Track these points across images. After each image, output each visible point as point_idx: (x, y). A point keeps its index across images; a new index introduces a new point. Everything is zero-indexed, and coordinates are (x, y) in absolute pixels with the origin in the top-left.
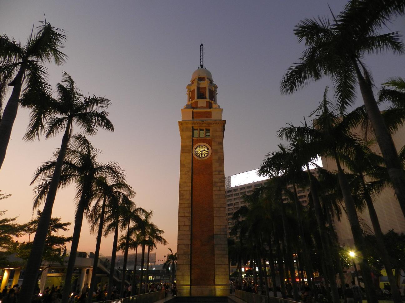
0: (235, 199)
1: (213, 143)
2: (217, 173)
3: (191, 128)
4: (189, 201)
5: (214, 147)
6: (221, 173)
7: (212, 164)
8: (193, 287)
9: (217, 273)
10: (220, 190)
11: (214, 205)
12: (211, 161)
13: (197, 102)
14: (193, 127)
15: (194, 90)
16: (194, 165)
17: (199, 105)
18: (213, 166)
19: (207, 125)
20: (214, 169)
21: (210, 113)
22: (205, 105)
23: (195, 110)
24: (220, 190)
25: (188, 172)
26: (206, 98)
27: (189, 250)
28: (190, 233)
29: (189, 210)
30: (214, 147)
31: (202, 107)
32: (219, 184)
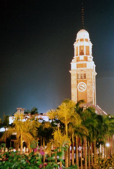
1: (87, 82)
2: (89, 98)
6: (91, 99)
7: (87, 94)
12: (87, 92)
16: (78, 95)
17: (80, 60)
20: (88, 97)
22: (83, 59)
23: (79, 63)
25: (76, 98)
31: (82, 60)
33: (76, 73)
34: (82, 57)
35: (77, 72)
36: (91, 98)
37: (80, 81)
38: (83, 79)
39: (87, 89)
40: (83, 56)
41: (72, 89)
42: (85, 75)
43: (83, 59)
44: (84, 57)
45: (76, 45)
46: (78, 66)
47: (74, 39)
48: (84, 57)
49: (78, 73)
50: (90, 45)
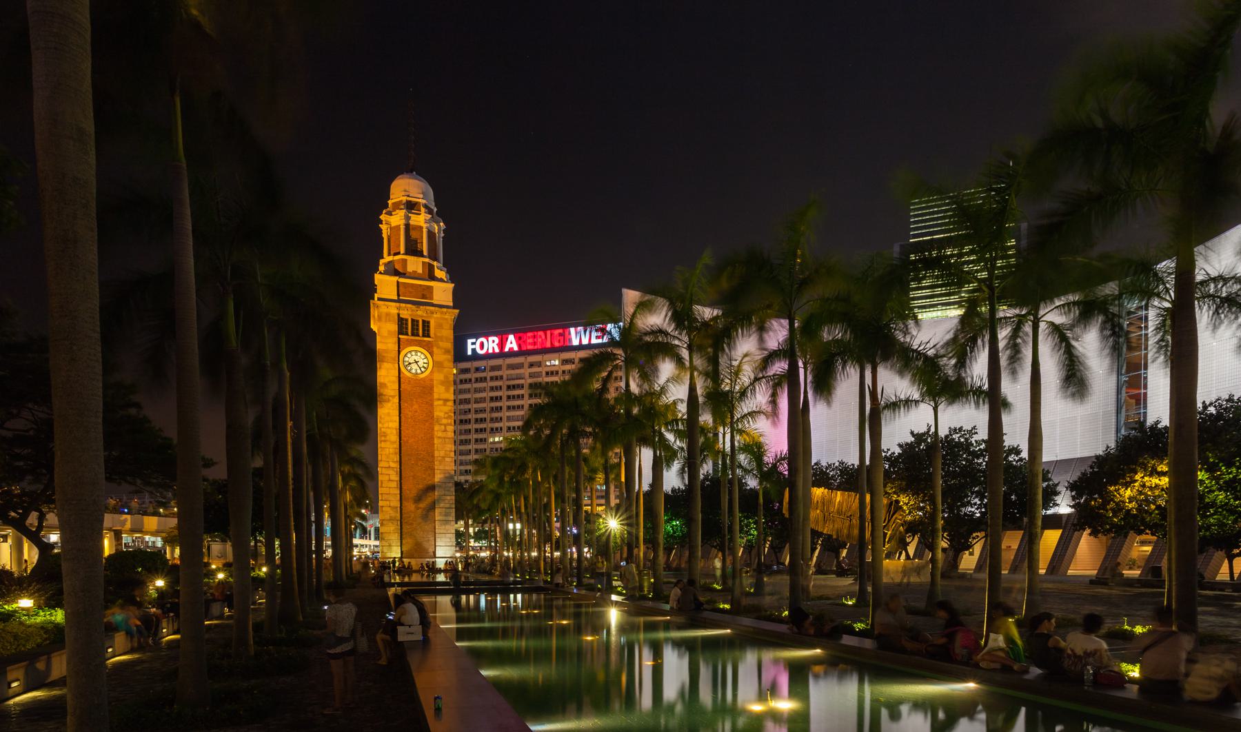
1: (435, 349)
2: (441, 402)
5: (436, 358)
10: (445, 431)
11: (436, 453)
12: (432, 380)
13: (405, 261)
15: (398, 227)
17: (410, 269)
18: (435, 390)
20: (436, 396)
22: (420, 271)
24: (445, 431)
26: (422, 256)
30: (436, 358)
32: (445, 421)
33: (396, 311)
34: (415, 264)
35: (398, 308)
36: (446, 400)
37: (411, 343)
39: (432, 372)
40: (422, 259)
42: (426, 324)
43: (420, 271)
48: (424, 263)
49: (405, 314)
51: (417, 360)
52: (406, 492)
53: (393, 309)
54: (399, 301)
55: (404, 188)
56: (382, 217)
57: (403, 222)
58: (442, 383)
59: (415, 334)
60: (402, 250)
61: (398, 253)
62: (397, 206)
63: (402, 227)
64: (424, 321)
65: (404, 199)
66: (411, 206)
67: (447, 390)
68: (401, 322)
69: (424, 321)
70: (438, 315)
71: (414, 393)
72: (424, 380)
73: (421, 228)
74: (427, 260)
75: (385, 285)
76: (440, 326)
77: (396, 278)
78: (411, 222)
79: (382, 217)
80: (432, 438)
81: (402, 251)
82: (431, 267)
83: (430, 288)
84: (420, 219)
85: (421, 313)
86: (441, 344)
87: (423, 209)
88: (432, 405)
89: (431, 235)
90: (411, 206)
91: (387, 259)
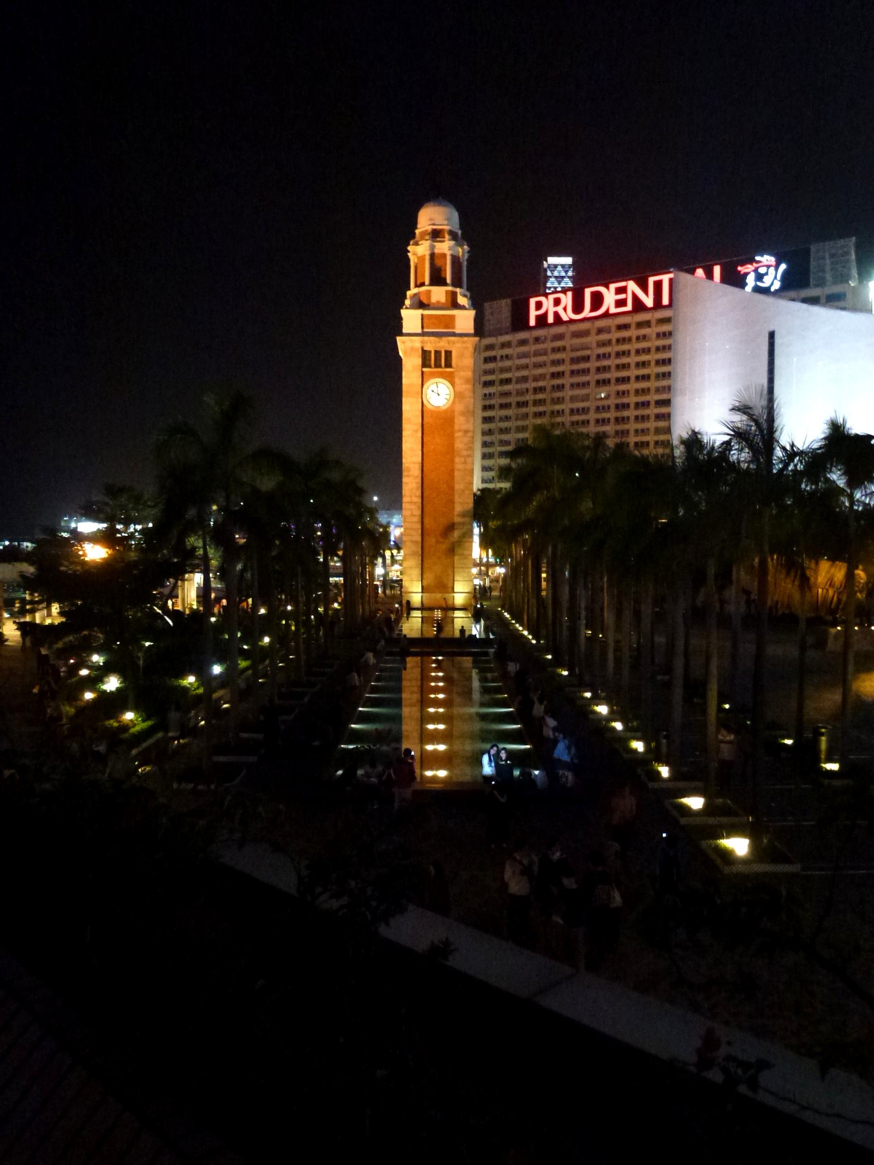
0: (518, 368)
1: (457, 381)
3: (420, 350)
4: (419, 480)
5: (458, 388)
8: (425, 594)
9: (456, 578)
10: (465, 463)
12: (453, 412)
13: (429, 292)
14: (422, 349)
19: (447, 345)
20: (456, 427)
21: (452, 318)
22: (443, 299)
24: (465, 463)
25: (416, 431)
27: (420, 550)
28: (420, 527)
29: (419, 493)
32: (465, 453)
34: (439, 294)
37: (433, 375)
38: (440, 366)
41: (404, 399)
42: (448, 354)
44: (447, 292)
45: (418, 251)
46: (425, 320)
47: (408, 234)
48: (447, 292)
50: (463, 251)
51: (439, 394)
52: (427, 525)
53: (417, 342)
54: (423, 334)
55: (430, 217)
56: (409, 248)
57: (427, 253)
58: (463, 414)
59: (438, 365)
60: (427, 282)
61: (423, 284)
62: (423, 234)
63: (427, 258)
64: (446, 352)
65: (430, 228)
66: (436, 235)
67: (468, 421)
68: (425, 354)
69: (446, 352)
70: (459, 345)
71: (436, 424)
72: (445, 411)
73: (444, 255)
74: (450, 288)
75: (411, 318)
76: (461, 356)
77: (420, 312)
78: (436, 251)
79: (409, 248)
80: (453, 471)
81: (427, 282)
82: (454, 295)
83: (452, 318)
84: (445, 247)
85: (443, 344)
86: (462, 374)
87: (447, 236)
88: (453, 436)
89: (455, 260)
90: (436, 235)
91: (413, 291)
